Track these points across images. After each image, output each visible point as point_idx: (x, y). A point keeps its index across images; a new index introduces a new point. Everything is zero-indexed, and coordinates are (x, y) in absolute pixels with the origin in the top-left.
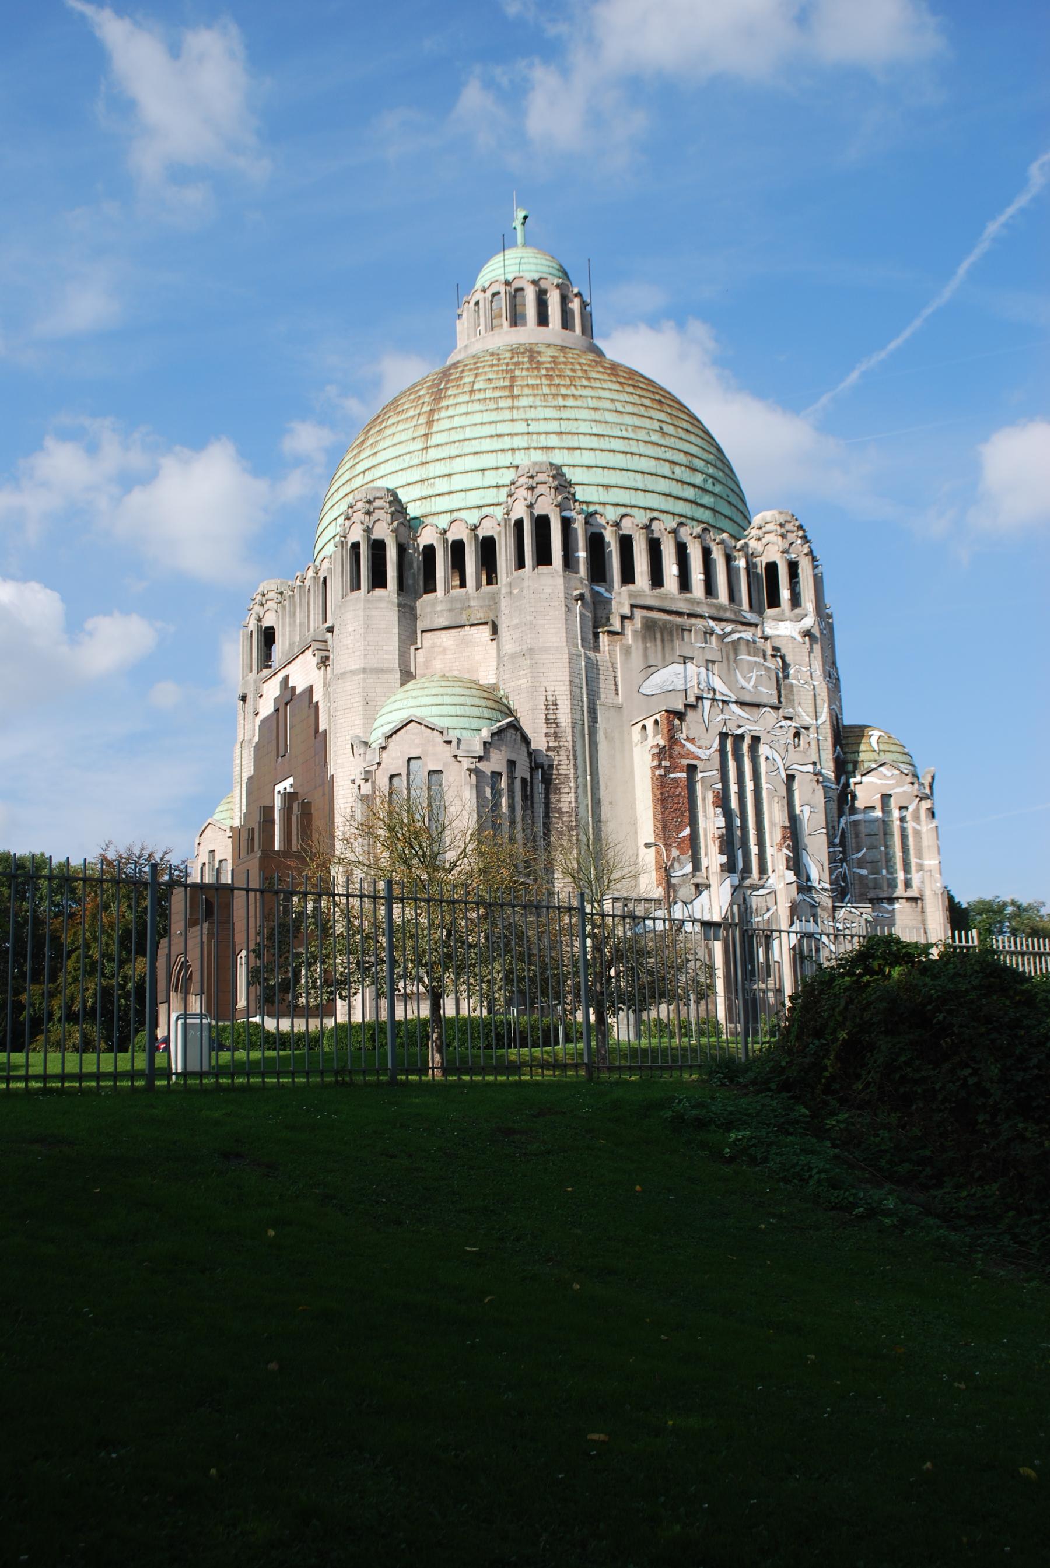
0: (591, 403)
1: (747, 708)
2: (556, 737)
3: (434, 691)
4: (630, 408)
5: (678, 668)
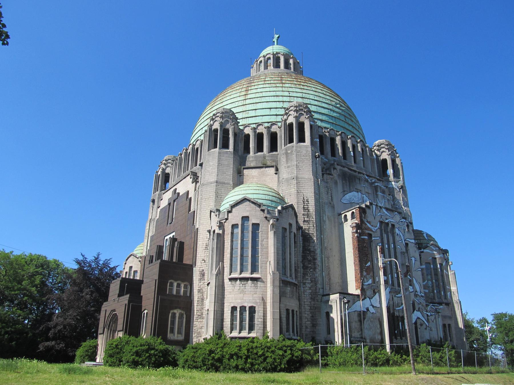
0: (314, 89)
2: (308, 216)
3: (255, 188)
4: (328, 94)
5: (355, 193)
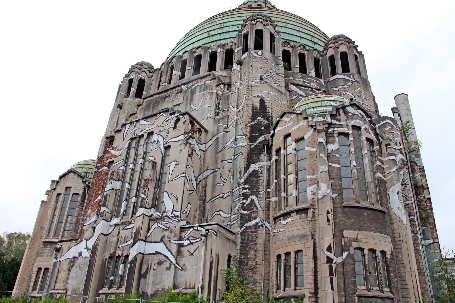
1: (149, 120)
